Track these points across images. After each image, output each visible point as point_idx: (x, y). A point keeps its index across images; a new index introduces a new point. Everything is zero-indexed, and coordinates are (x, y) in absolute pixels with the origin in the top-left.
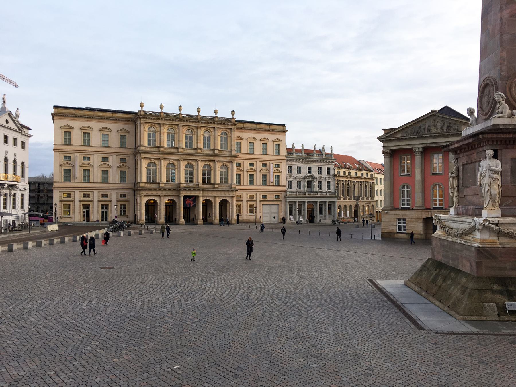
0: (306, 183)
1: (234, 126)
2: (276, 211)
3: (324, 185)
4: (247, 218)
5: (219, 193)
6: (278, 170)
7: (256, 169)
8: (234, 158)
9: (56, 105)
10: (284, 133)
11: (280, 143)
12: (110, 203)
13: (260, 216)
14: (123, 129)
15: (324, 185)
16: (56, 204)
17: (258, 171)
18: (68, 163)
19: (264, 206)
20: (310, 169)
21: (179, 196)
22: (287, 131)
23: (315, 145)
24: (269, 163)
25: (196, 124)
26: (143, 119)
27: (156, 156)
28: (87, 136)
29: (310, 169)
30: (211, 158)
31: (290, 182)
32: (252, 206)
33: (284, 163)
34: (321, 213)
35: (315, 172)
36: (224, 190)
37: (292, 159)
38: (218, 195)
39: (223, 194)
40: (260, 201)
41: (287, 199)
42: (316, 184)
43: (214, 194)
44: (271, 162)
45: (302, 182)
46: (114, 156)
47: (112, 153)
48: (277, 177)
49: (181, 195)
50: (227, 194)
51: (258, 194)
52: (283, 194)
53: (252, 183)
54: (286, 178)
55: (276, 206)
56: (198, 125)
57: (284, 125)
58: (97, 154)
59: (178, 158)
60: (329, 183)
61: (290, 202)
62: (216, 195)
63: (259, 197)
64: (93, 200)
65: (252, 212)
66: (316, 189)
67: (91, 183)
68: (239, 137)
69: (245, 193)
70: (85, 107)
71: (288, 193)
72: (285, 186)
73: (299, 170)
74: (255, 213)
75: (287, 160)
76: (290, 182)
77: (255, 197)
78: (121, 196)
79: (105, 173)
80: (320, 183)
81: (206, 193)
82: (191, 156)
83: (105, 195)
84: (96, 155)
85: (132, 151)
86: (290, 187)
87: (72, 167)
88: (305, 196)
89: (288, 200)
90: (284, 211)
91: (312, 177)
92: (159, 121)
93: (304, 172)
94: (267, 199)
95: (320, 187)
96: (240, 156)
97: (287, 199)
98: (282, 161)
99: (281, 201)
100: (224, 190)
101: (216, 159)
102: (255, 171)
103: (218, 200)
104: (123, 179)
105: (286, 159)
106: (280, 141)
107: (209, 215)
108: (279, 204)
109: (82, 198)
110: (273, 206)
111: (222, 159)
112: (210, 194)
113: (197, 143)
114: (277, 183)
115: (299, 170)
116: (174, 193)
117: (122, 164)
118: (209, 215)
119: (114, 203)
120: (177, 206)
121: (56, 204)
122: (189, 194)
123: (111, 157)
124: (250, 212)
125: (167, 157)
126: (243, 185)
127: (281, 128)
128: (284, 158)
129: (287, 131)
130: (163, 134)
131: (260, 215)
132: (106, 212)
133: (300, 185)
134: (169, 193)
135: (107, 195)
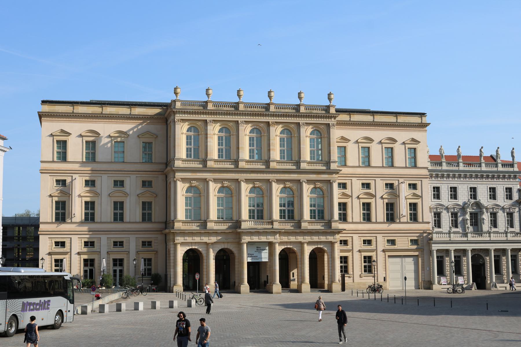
0: (468, 217)
1: (333, 119)
3: (502, 218)
4: (360, 281)
6: (414, 195)
7: (374, 194)
8: (334, 175)
9: (45, 99)
10: (425, 129)
13: (384, 278)
15: (502, 218)
16: (42, 259)
17: (378, 196)
20: (473, 190)
21: (239, 244)
23: (482, 148)
26: (178, 115)
29: (473, 190)
31: (438, 215)
32: (368, 260)
33: (426, 182)
34: (498, 270)
35: (483, 197)
41: (433, 245)
42: (486, 217)
44: (401, 180)
45: (459, 214)
46: (133, 177)
49: (243, 241)
51: (380, 237)
53: (367, 218)
54: (430, 208)
56: (270, 121)
57: (422, 115)
60: (510, 215)
61: (438, 251)
62: (303, 241)
63: (381, 243)
64: (100, 252)
65: (370, 271)
66: (486, 226)
70: (88, 100)
72: (428, 223)
73: (454, 193)
74: (374, 273)
75: (431, 176)
76: (438, 215)
78: (144, 244)
79: (119, 206)
80: (494, 215)
83: (118, 244)
84: (105, 177)
85: (162, 167)
86: (438, 223)
88: (465, 239)
91: (478, 205)
93: (464, 196)
95: (494, 223)
96: (345, 170)
97: (433, 245)
98: (421, 177)
101: (303, 177)
103: (308, 250)
104: (146, 217)
105: (428, 173)
107: (293, 277)
114: (414, 218)
115: (454, 193)
117: (145, 189)
118: (293, 277)
119: (133, 255)
120: (236, 260)
121: (42, 259)
122: (255, 239)
123: (128, 179)
124: (365, 271)
126: (353, 223)
128: (425, 172)
131: (385, 276)
132: (121, 271)
133: (456, 221)
135: (121, 244)
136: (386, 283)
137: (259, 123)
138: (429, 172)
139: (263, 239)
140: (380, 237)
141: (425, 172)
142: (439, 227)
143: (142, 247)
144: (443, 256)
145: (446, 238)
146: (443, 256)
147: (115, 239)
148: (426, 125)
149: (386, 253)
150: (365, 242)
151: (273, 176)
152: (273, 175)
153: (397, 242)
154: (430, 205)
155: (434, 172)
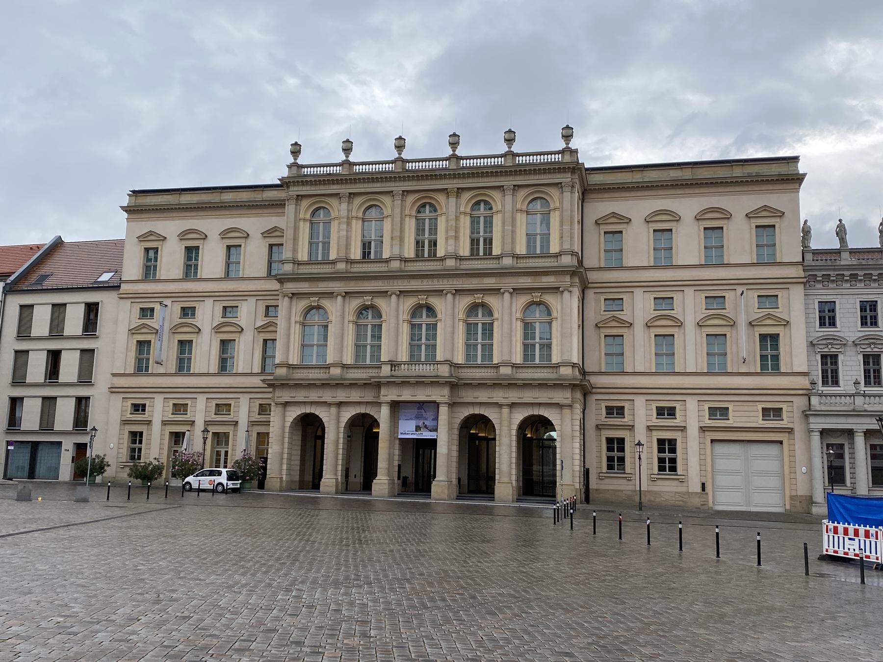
1: (569, 175)
2: (773, 466)
5: (514, 396)
11: (778, 220)
12: (232, 428)
13: (703, 485)
14: (275, 229)
16: (94, 429)
18: (144, 326)
19: (720, 449)
22: (805, 175)
24: (733, 293)
25: (443, 182)
27: (323, 287)
28: (192, 252)
30: (489, 282)
32: (667, 446)
36: (527, 385)
37: (831, 273)
38: (509, 401)
39: (528, 396)
40: (703, 429)
41: (812, 419)
43: (499, 396)
44: (739, 290)
46: (252, 301)
47: (244, 296)
48: (770, 341)
50: (543, 396)
52: (800, 403)
54: (812, 344)
55: (773, 450)
58: (212, 300)
59: (384, 289)
61: (823, 433)
62: (501, 400)
67: (194, 375)
68: (614, 215)
69: (640, 401)
71: (815, 400)
77: (678, 413)
81: (469, 396)
82: (425, 282)
84: (209, 302)
86: (831, 376)
87: (153, 336)
89: (818, 424)
90: (804, 469)
92: (339, 187)
94: (730, 423)
98: (786, 283)
99: (790, 431)
100: (527, 385)
102: (680, 325)
105: (802, 274)
106: (782, 214)
108: (781, 442)
109: (214, 416)
110: (755, 450)
111: (525, 282)
112: (483, 396)
113: (447, 239)
116: (369, 396)
117: (268, 320)
119: (199, 426)
122: (406, 395)
123: (244, 303)
125: (352, 287)
127: (782, 169)
129: (805, 175)
130: (349, 224)
134: (355, 395)
136: (707, 494)
137: (431, 193)
138: (804, 270)
139: (422, 395)
140: (692, 403)
141: (796, 272)
142: (836, 383)
143: (259, 414)
144: (844, 444)
145: (843, 404)
146: (844, 444)
147: (218, 400)
148: (798, 179)
149: (707, 433)
150: (660, 412)
151: (449, 283)
152: (451, 281)
153: (731, 414)
154: (811, 339)
155: (820, 270)
